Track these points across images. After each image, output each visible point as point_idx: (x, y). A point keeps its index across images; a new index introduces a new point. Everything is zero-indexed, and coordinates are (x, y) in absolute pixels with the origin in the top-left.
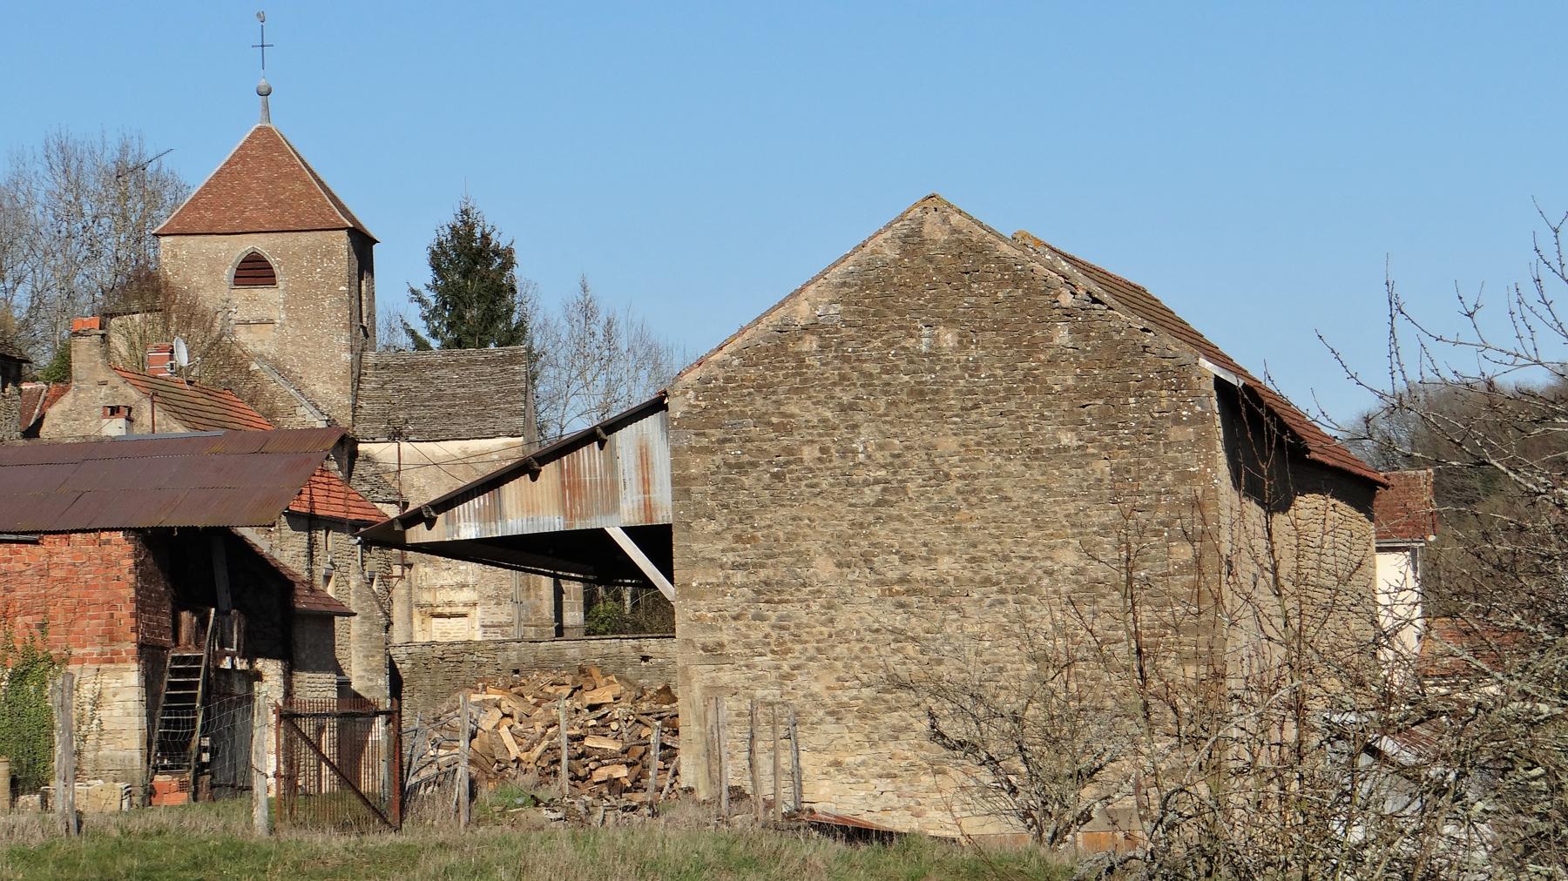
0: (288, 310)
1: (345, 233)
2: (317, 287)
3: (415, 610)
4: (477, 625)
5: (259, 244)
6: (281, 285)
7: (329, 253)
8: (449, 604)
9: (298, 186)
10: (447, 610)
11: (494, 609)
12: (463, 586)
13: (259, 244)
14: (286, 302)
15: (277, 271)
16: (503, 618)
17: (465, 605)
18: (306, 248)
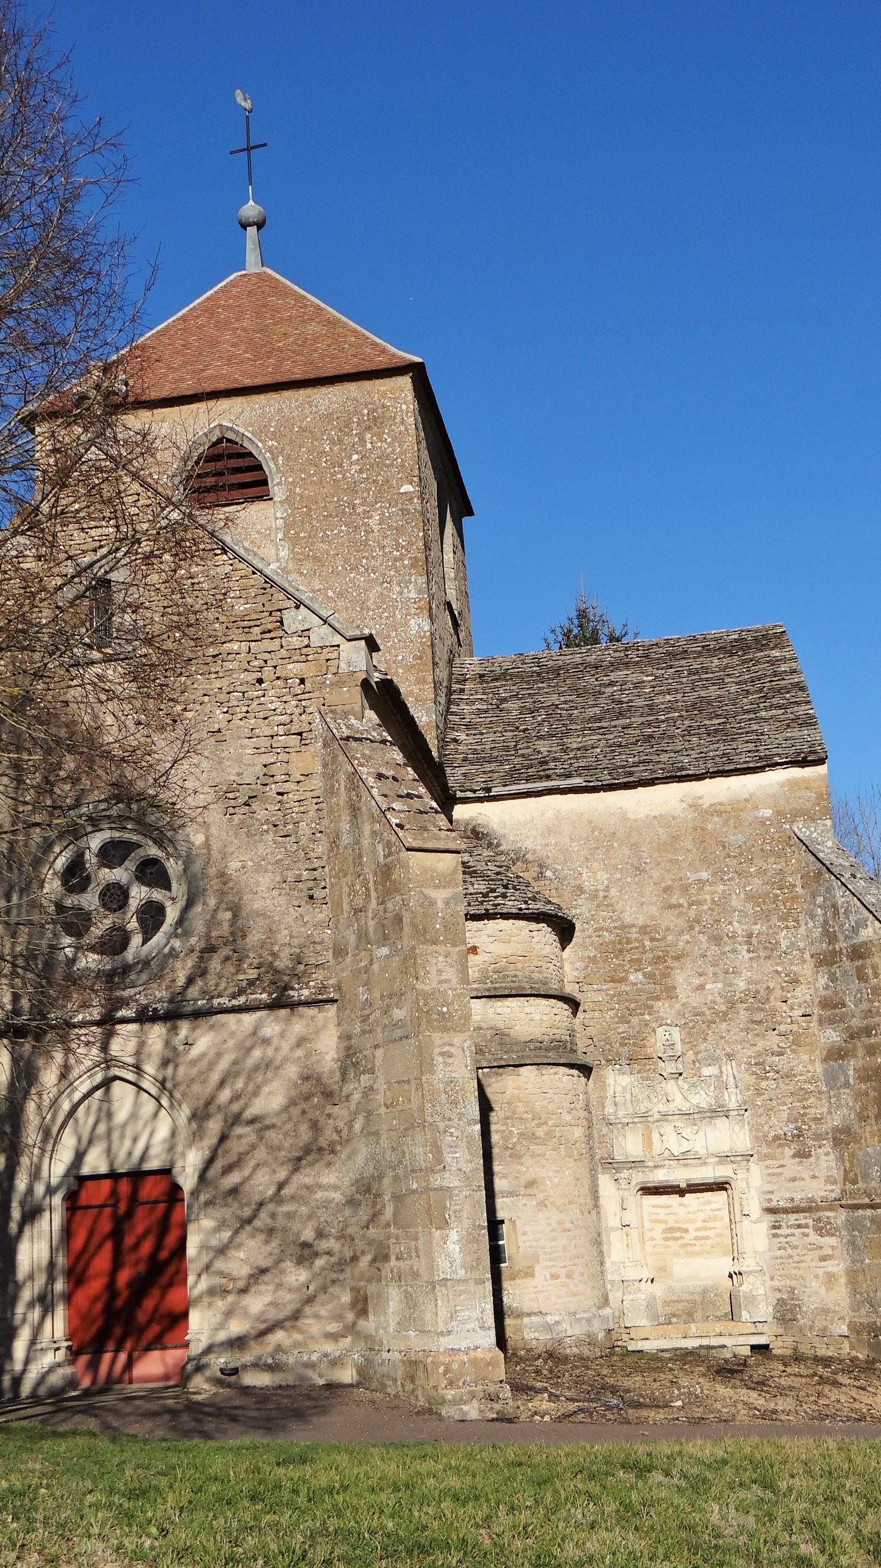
0: (294, 541)
1: (405, 382)
2: (353, 489)
3: (605, 1182)
4: (754, 1207)
5: (236, 417)
6: (278, 492)
7: (376, 421)
8: (684, 1158)
9: (312, 328)
10: (680, 1176)
11: (793, 1167)
12: (717, 1112)
13: (236, 417)
14: (288, 526)
15: (269, 467)
16: (818, 1190)
17: (724, 1158)
18: (329, 416)
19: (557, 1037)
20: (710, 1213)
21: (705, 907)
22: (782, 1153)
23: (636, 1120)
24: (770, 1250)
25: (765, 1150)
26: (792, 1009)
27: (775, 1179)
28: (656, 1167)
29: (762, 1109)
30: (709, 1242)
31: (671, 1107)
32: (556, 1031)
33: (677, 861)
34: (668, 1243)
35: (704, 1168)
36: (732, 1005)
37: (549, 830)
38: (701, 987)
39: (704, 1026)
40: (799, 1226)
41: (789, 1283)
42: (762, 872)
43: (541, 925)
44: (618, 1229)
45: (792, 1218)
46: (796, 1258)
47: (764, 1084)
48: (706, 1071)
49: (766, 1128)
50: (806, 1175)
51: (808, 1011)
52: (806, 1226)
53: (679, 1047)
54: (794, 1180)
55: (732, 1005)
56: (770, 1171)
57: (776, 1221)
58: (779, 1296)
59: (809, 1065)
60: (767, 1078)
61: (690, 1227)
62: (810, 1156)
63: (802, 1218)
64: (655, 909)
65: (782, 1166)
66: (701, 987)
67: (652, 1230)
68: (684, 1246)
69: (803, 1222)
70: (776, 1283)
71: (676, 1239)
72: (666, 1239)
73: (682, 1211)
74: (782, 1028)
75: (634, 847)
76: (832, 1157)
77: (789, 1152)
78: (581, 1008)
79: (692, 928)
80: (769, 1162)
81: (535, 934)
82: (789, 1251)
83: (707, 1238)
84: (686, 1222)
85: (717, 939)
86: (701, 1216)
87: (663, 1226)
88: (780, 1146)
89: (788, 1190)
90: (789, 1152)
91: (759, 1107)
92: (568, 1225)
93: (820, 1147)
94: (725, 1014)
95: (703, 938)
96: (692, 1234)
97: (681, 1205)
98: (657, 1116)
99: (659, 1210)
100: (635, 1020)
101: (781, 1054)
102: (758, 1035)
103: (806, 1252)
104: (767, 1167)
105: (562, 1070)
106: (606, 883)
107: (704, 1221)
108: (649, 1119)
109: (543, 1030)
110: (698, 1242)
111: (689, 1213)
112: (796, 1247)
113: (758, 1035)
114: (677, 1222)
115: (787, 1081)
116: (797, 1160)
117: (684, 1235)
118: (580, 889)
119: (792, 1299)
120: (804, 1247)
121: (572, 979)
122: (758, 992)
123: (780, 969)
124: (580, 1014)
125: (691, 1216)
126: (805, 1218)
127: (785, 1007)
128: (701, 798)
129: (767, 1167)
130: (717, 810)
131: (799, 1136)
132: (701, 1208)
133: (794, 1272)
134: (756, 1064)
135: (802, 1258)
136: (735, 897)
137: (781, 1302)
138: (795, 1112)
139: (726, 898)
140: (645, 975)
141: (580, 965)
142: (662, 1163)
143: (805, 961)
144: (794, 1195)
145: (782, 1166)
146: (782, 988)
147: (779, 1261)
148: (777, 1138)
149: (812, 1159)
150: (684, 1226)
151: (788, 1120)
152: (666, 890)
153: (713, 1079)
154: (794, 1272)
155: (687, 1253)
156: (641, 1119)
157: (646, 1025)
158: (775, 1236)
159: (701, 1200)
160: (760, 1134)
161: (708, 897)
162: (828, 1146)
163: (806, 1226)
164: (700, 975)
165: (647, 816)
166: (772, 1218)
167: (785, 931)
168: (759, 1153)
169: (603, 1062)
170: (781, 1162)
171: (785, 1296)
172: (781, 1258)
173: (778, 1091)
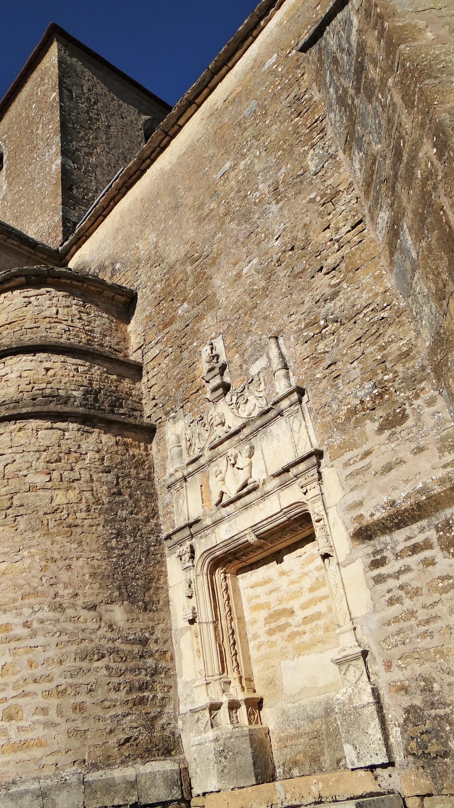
12: (270, 414)
19: (48, 391)
20: (316, 574)
21: (232, 195)
22: (363, 434)
23: (191, 469)
24: (375, 611)
25: (338, 439)
26: (338, 229)
27: (359, 480)
28: (216, 523)
29: (325, 381)
30: (321, 622)
31: (220, 432)
32: (44, 385)
33: (204, 174)
34: (273, 638)
35: (268, 502)
36: (270, 275)
37: (118, 230)
38: (239, 276)
39: (247, 318)
40: (415, 549)
41: (418, 669)
42: (277, 115)
43: (43, 290)
44: (187, 629)
45: (400, 538)
46: (422, 615)
47: (321, 347)
48: (254, 370)
49: (335, 407)
50: (405, 452)
51: (357, 219)
52: (427, 545)
53: (223, 359)
54: (388, 468)
55: (270, 275)
56: (351, 469)
57: (375, 553)
58: (406, 701)
59: (375, 283)
60: (323, 337)
61: (295, 604)
62: (404, 417)
63: (417, 532)
64: (192, 231)
65: (367, 454)
66: (239, 276)
67: (254, 622)
68: (292, 636)
69: (420, 539)
70: (398, 675)
71: (282, 628)
72: (271, 632)
73: (284, 582)
74: (331, 261)
75: (173, 192)
76: (441, 403)
77: (371, 427)
78: (144, 372)
79: (223, 223)
80: (348, 456)
81: (32, 299)
82: (408, 603)
83: (318, 616)
84: (291, 598)
85: (246, 217)
86: (307, 583)
87: (264, 613)
88: (358, 422)
89: (383, 490)
90: (371, 427)
91: (320, 380)
92: (20, 631)
93: (417, 396)
94: (265, 289)
95: (233, 225)
96: (300, 615)
97: (282, 574)
98: (207, 454)
99: (259, 590)
100: (185, 354)
101: (335, 295)
102: (303, 289)
103: (436, 596)
104: (346, 465)
105: (33, 423)
106: (155, 240)
107: (312, 590)
108: (202, 461)
109: (23, 387)
110: (307, 628)
111: (292, 582)
112: (417, 592)
113: (303, 289)
114: (280, 601)
115: (350, 325)
116: (387, 433)
117: (290, 620)
118: (139, 261)
119: (433, 705)
120: (432, 588)
121: (135, 347)
122: (295, 239)
123: (312, 196)
124: (144, 379)
125: (295, 587)
126: (422, 530)
127: (328, 234)
128: (215, 104)
129: (346, 465)
130: (231, 101)
131: (381, 395)
132: (306, 570)
133: (422, 643)
134: (307, 326)
135: (433, 612)
136: (256, 161)
137: (412, 714)
138: (370, 362)
139: (249, 168)
140: (189, 303)
141: (141, 329)
142: (218, 516)
143: (338, 165)
144: (395, 496)
145: (367, 454)
146: (321, 215)
147: (394, 627)
148: (353, 411)
149: (410, 422)
150: (287, 605)
151: (363, 380)
152: (199, 208)
153: (261, 375)
154: (422, 643)
155: (296, 648)
156: (194, 466)
157: (194, 353)
158: (379, 579)
159: (304, 557)
160: (329, 418)
161: (233, 183)
162: (429, 389)
163: (427, 545)
164: (235, 265)
165: (179, 158)
166: (366, 549)
167: (311, 152)
168: (329, 447)
169: (164, 417)
170: (365, 448)
171: (418, 701)
172: (396, 620)
173: (341, 345)
